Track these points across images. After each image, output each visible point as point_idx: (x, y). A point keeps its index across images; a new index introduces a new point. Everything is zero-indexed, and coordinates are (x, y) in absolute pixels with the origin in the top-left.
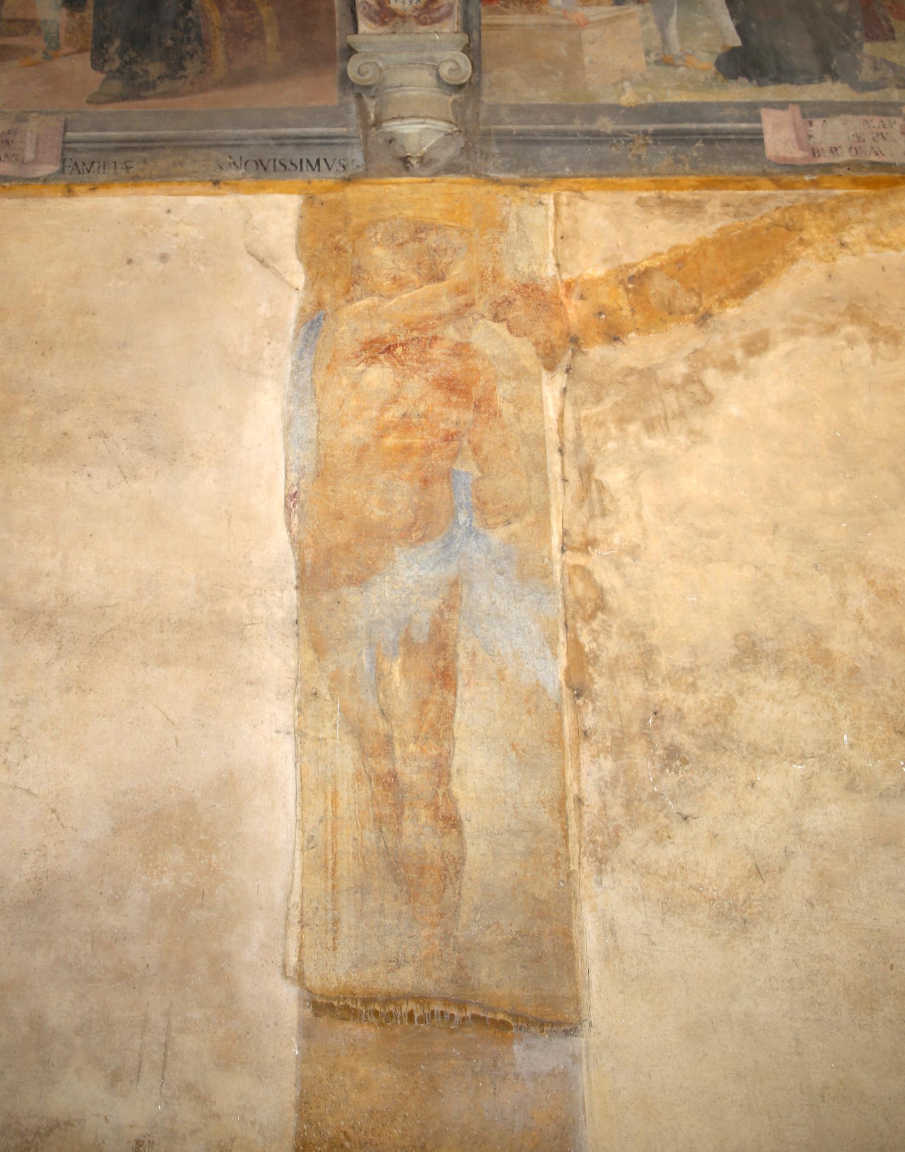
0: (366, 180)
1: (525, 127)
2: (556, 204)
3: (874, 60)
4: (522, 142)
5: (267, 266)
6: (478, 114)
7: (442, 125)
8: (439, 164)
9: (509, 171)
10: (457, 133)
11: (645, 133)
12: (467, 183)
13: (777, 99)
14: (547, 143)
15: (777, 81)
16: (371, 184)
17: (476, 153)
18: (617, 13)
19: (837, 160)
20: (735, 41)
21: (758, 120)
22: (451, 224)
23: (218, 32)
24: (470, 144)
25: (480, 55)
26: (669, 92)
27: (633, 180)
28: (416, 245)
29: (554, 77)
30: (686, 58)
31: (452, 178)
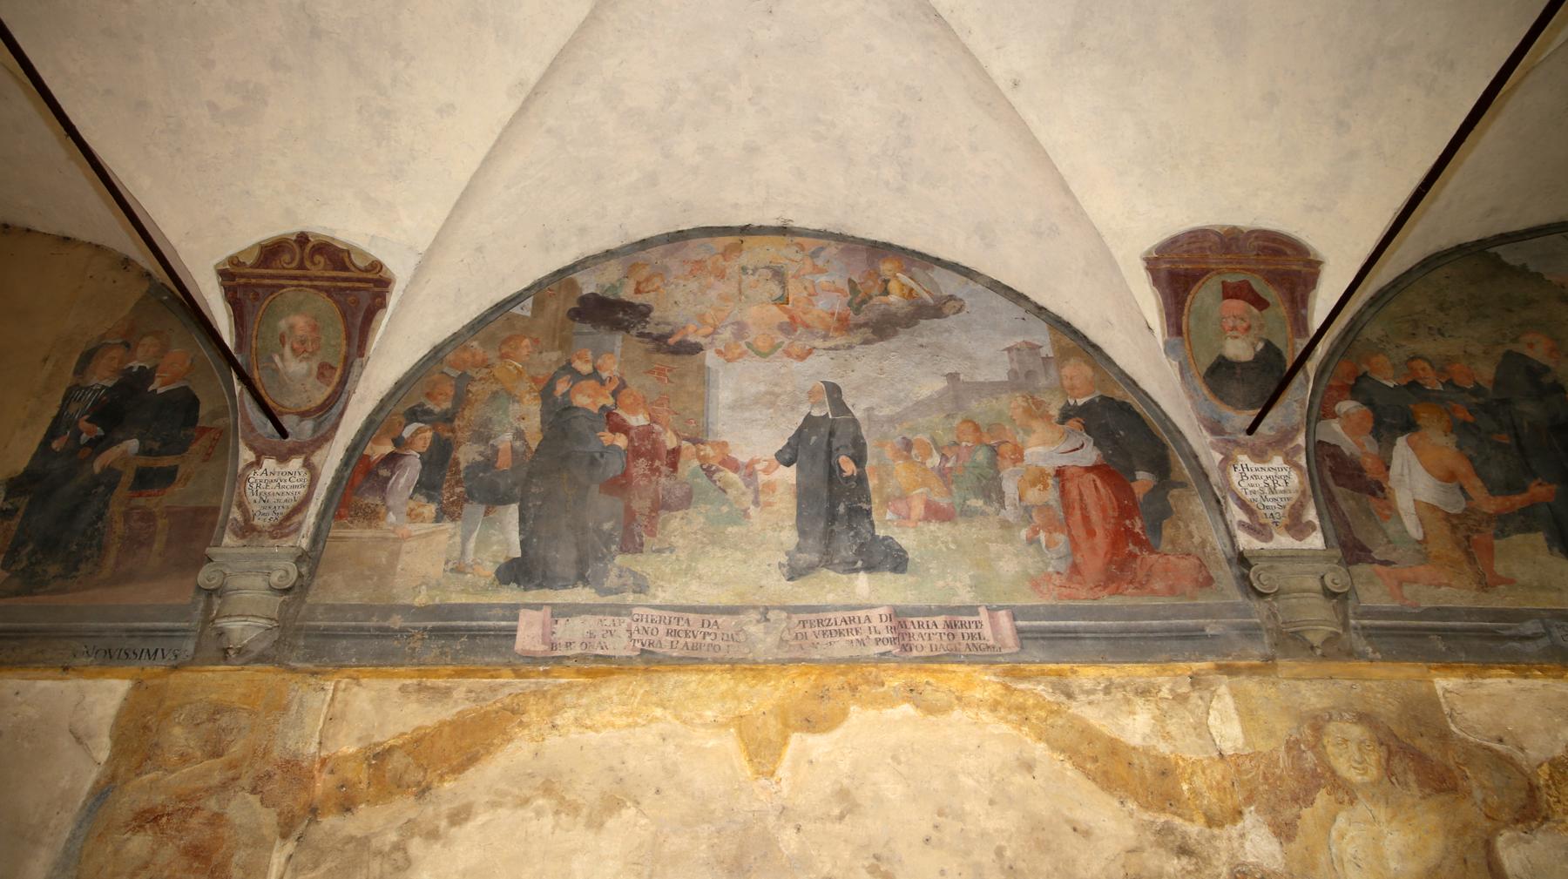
0: (190, 668)
1: (332, 624)
2: (335, 690)
3: (620, 569)
4: (324, 636)
5: (81, 743)
7: (262, 622)
8: (253, 654)
9: (307, 661)
11: (425, 629)
12: (269, 672)
14: (344, 637)
15: (540, 586)
16: (192, 671)
19: (569, 653)
20: (516, 552)
21: (516, 619)
22: (245, 707)
23: (117, 540)
27: (402, 669)
28: (210, 725)
29: (369, 582)
31: (259, 666)
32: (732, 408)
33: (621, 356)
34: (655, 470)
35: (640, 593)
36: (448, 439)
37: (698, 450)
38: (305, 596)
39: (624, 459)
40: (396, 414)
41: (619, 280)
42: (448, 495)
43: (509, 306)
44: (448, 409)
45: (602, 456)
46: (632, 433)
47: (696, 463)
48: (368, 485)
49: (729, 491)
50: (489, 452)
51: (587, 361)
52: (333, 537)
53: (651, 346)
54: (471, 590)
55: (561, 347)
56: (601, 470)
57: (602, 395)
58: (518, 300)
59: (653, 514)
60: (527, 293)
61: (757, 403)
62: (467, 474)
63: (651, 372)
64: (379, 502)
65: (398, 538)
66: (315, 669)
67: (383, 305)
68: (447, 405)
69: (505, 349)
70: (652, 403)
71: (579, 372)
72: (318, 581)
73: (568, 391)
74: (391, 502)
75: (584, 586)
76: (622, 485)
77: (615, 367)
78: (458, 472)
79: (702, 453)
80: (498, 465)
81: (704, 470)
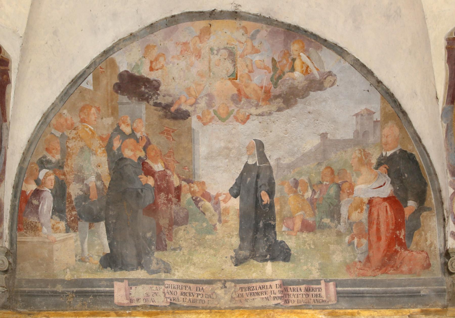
1: (31, 289)
3: (157, 259)
4: (29, 295)
6: (14, 283)
9: (24, 308)
10: (6, 292)
11: (73, 292)
14: (38, 296)
15: (121, 269)
17: (13, 300)
19: (139, 304)
20: (108, 251)
21: (113, 286)
24: (11, 297)
25: (16, 256)
27: (67, 312)
29: (42, 266)
31: (4, 311)
66: (29, 312)
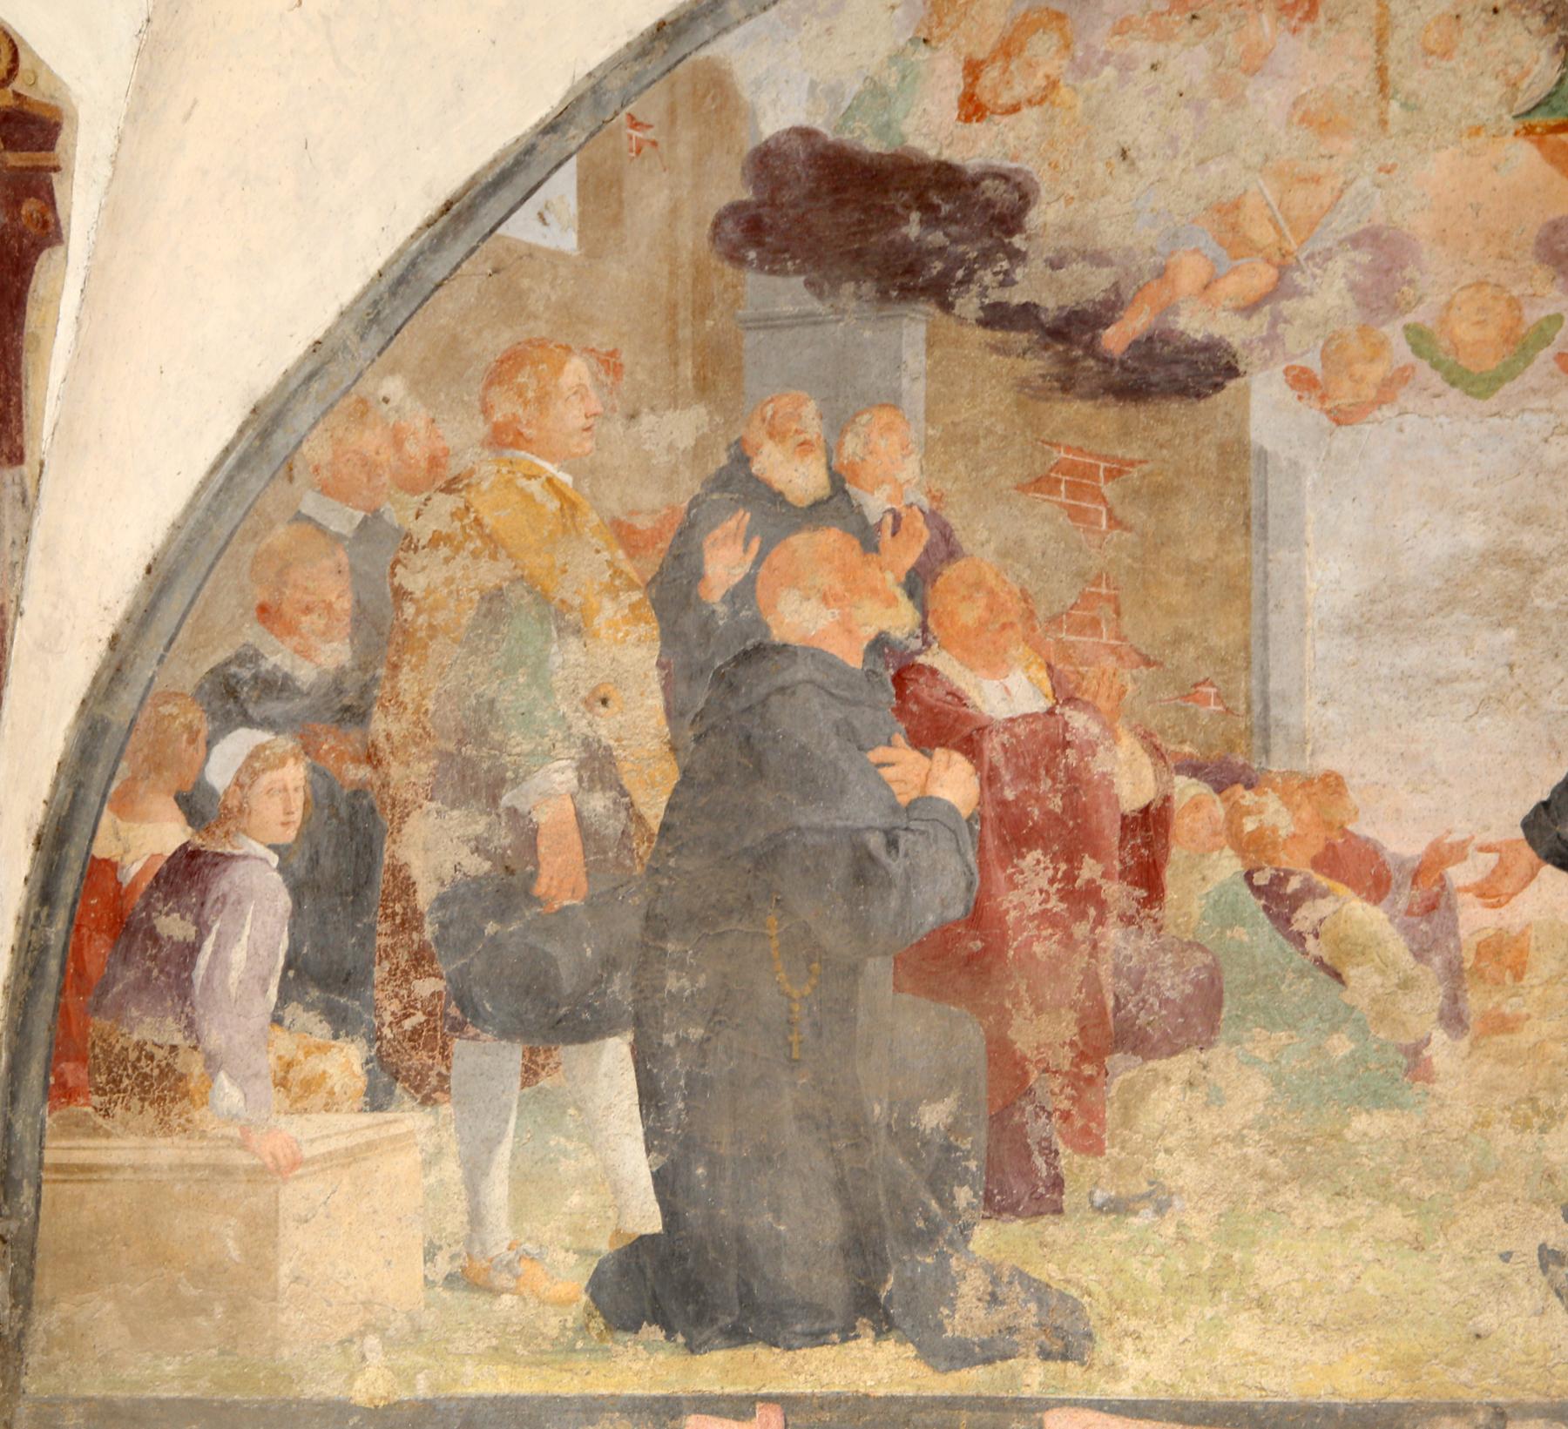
13: (729, 1390)
15: (737, 1336)
18: (370, 1134)
20: (647, 1218)
26: (469, 1368)
29: (201, 1321)
30: (522, 1267)
32: (1356, 628)
33: (930, 417)
34: (1082, 898)
35: (1065, 1357)
36: (359, 792)
37: (1236, 813)
38: (18, 1374)
39: (971, 857)
40: (168, 697)
41: (896, 57)
42: (395, 1006)
43: (494, 208)
44: (341, 671)
45: (892, 844)
46: (993, 748)
47: (1227, 866)
48: (131, 975)
49: (1351, 973)
50: (504, 839)
51: (805, 446)
52: (58, 1168)
53: (1036, 366)
54: (520, 1349)
55: (703, 387)
56: (894, 903)
57: (874, 592)
58: (523, 181)
59: (1088, 1070)
60: (551, 147)
61: (1450, 604)
62: (444, 926)
63: (1042, 483)
64: (178, 1039)
65: (263, 1169)
67: (49, 233)
68: (335, 654)
69: (505, 407)
70: (1054, 620)
71: (777, 497)
72: (45, 1322)
73: (750, 580)
74: (214, 1038)
75: (880, 1335)
76: (972, 958)
77: (910, 469)
78: (410, 922)
79: (1250, 825)
80: (540, 888)
81: (1257, 891)
